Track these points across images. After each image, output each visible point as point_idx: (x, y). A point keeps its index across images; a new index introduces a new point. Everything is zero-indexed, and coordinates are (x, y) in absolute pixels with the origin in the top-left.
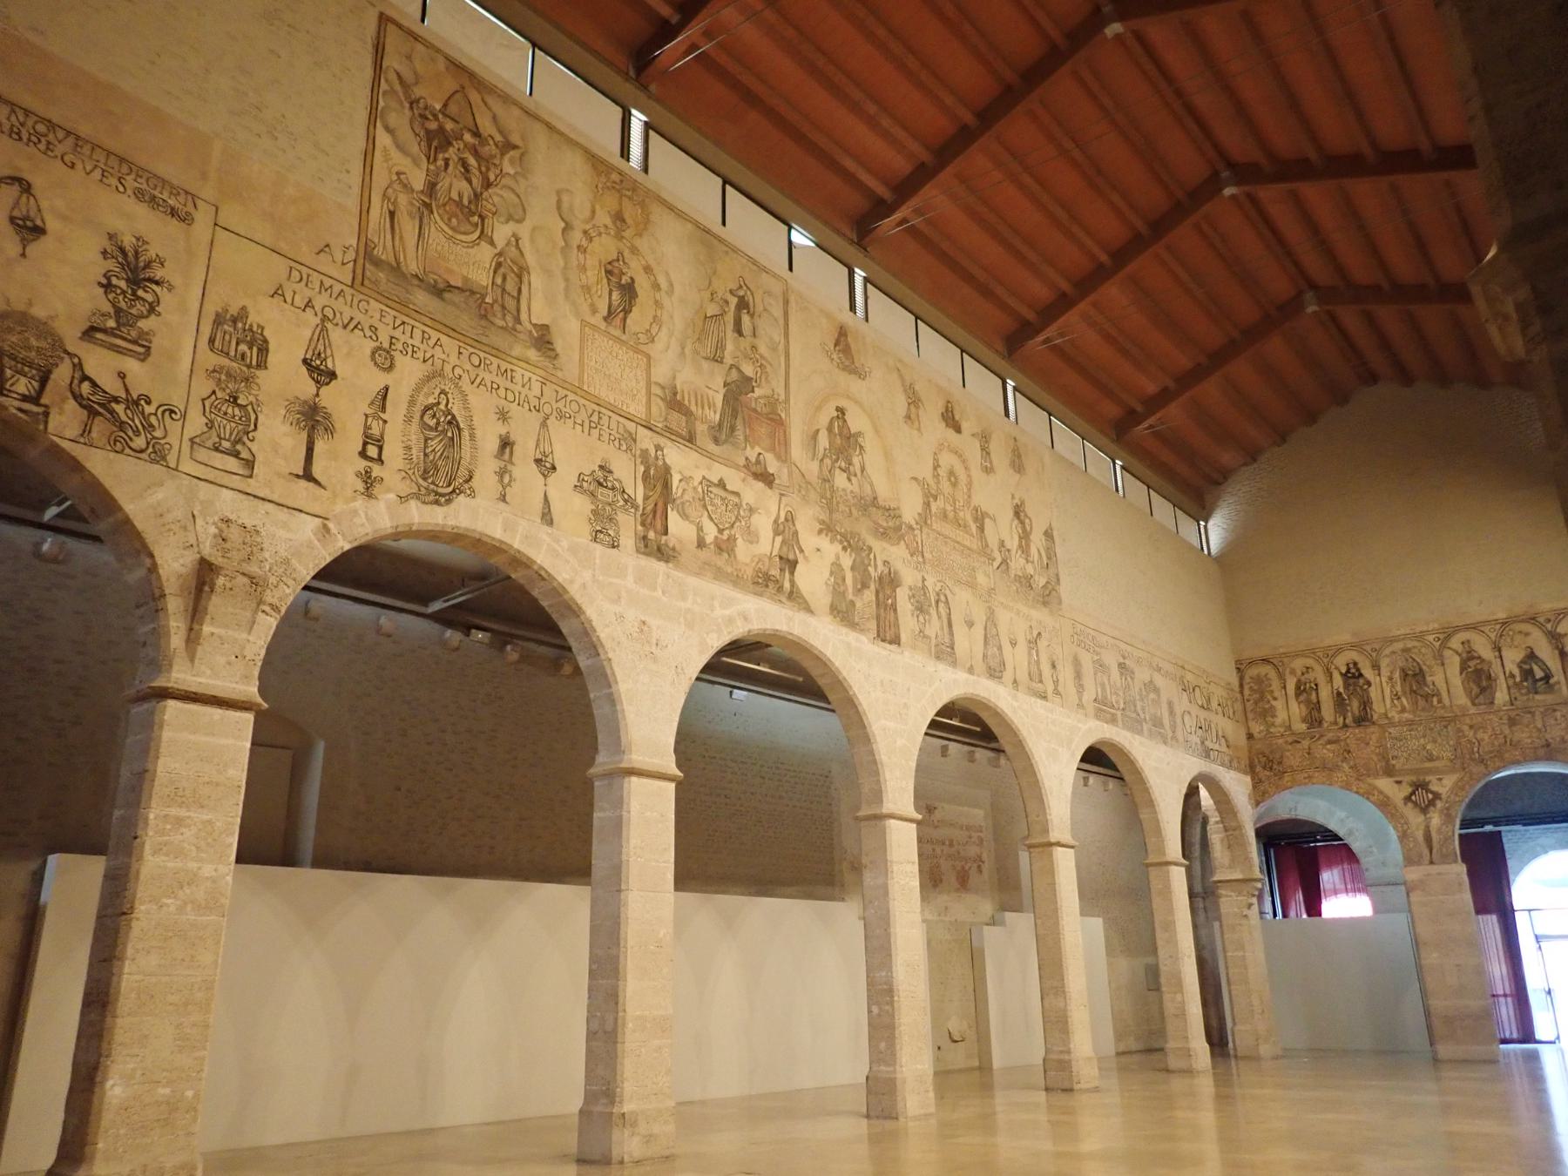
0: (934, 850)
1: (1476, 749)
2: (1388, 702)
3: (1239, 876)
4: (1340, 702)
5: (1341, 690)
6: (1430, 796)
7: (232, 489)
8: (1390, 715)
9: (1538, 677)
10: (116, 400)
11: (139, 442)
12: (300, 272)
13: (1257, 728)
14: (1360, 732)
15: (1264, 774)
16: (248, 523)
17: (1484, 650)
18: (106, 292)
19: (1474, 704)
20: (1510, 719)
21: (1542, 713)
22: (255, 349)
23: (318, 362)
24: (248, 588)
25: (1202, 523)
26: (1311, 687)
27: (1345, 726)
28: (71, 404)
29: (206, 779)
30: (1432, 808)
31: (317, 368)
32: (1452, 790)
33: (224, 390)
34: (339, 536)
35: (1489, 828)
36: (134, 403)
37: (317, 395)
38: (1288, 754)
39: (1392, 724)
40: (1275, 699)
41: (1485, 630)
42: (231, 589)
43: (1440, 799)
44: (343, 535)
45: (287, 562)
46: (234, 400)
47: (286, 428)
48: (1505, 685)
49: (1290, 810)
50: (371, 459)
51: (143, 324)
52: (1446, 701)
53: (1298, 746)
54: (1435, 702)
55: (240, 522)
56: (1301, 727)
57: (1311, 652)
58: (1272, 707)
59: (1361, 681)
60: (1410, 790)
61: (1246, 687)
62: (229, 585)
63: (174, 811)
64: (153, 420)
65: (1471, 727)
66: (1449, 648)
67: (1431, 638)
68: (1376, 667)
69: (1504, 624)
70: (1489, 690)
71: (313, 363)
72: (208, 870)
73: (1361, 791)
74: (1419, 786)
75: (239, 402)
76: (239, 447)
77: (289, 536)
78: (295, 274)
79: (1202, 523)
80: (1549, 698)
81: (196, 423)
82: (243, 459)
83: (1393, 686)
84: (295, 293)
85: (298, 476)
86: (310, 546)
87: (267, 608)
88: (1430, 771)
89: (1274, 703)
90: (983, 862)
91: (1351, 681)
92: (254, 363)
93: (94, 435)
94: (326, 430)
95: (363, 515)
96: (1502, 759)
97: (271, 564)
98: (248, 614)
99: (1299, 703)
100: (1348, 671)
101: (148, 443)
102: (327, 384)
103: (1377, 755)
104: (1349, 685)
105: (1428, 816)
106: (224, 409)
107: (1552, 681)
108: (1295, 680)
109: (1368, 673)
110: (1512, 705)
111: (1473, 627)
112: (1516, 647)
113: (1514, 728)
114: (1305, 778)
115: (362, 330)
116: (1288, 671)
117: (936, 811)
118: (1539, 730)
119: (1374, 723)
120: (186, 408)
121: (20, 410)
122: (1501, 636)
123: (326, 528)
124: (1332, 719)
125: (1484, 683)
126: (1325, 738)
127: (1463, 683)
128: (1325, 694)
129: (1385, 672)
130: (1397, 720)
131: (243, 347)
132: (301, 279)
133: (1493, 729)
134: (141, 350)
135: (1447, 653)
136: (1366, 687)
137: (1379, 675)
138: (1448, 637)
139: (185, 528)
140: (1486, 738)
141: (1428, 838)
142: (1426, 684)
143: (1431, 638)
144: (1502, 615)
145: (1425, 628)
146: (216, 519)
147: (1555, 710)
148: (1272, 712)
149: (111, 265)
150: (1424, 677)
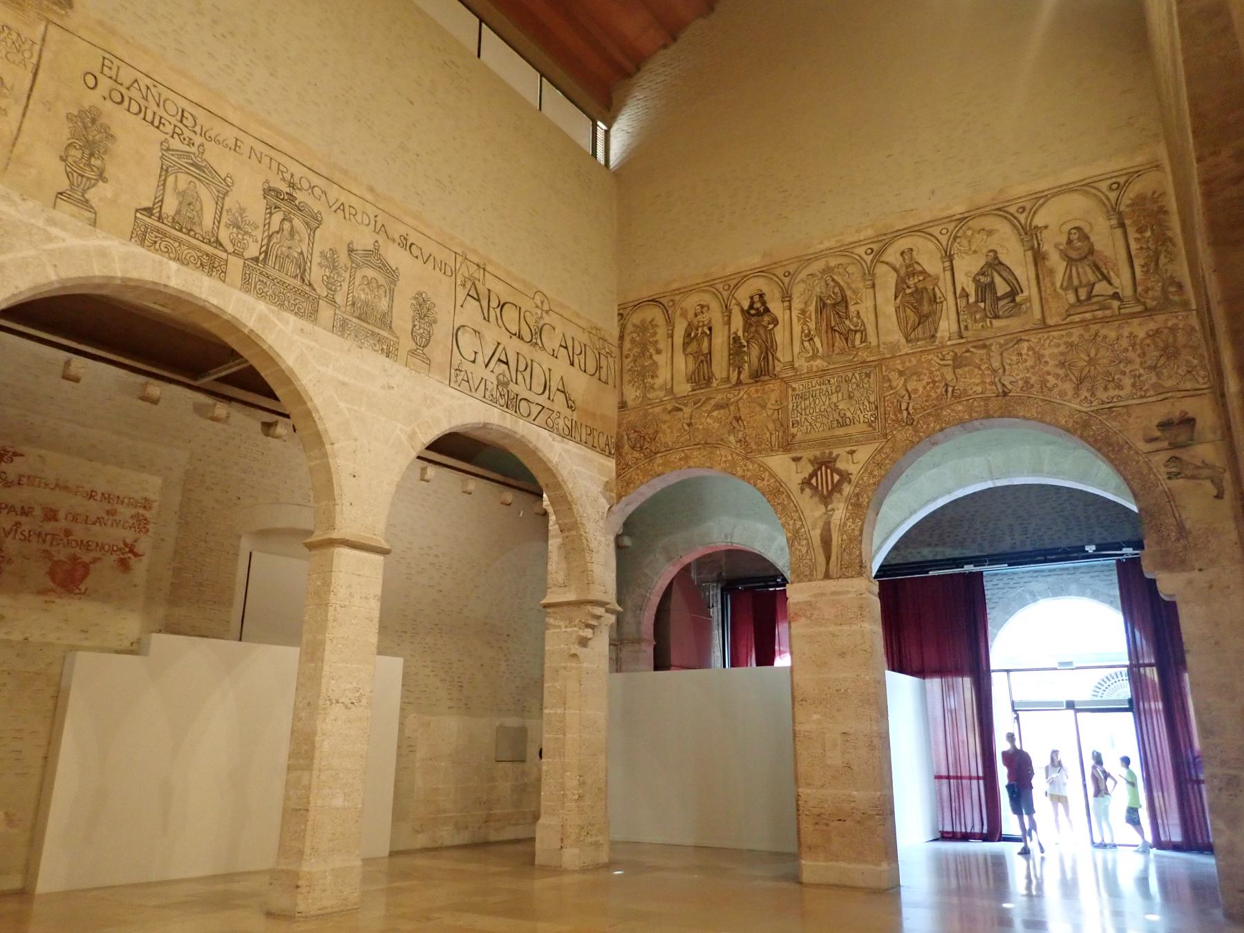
1: (904, 406)
2: (797, 349)
3: (571, 597)
4: (736, 349)
5: (740, 333)
6: (836, 477)
8: (796, 365)
9: (999, 294)
13: (632, 394)
14: (757, 391)
15: (631, 456)
17: (931, 262)
19: (908, 341)
20: (955, 358)
21: (1001, 346)
25: (601, 126)
26: (703, 332)
27: (739, 382)
30: (836, 495)
32: (865, 467)
35: (969, 568)
38: (664, 427)
39: (798, 376)
40: (659, 352)
41: (935, 231)
43: (850, 482)
48: (953, 309)
49: (726, 537)
52: (872, 339)
53: (680, 414)
54: (857, 342)
56: (684, 388)
57: (709, 285)
58: (655, 363)
59: (766, 318)
60: (810, 469)
61: (627, 339)
65: (901, 373)
66: (883, 262)
67: (861, 251)
68: (787, 297)
69: (960, 220)
70: (930, 319)
73: (749, 474)
74: (822, 464)
79: (601, 126)
80: (1014, 324)
83: (805, 323)
88: (840, 441)
89: (655, 357)
90: (136, 555)
91: (754, 319)
96: (938, 417)
99: (686, 355)
100: (751, 307)
103: (774, 421)
104: (751, 325)
105: (830, 507)
107: (1018, 299)
108: (685, 324)
109: (776, 307)
110: (962, 338)
111: (918, 230)
112: (975, 252)
113: (959, 371)
114: (680, 459)
116: (678, 312)
117: (17, 459)
118: (995, 371)
119: (775, 377)
122: (955, 238)
124: (724, 375)
125: (926, 308)
126: (713, 402)
127: (897, 309)
128: (720, 341)
129: (797, 305)
130: (805, 371)
133: (931, 372)
135: (881, 269)
136: (771, 326)
137: (790, 309)
138: (882, 251)
140: (921, 390)
141: (826, 542)
142: (847, 317)
143: (861, 251)
144: (959, 209)
145: (855, 239)
147: (1020, 340)
148: (653, 370)
150: (847, 307)
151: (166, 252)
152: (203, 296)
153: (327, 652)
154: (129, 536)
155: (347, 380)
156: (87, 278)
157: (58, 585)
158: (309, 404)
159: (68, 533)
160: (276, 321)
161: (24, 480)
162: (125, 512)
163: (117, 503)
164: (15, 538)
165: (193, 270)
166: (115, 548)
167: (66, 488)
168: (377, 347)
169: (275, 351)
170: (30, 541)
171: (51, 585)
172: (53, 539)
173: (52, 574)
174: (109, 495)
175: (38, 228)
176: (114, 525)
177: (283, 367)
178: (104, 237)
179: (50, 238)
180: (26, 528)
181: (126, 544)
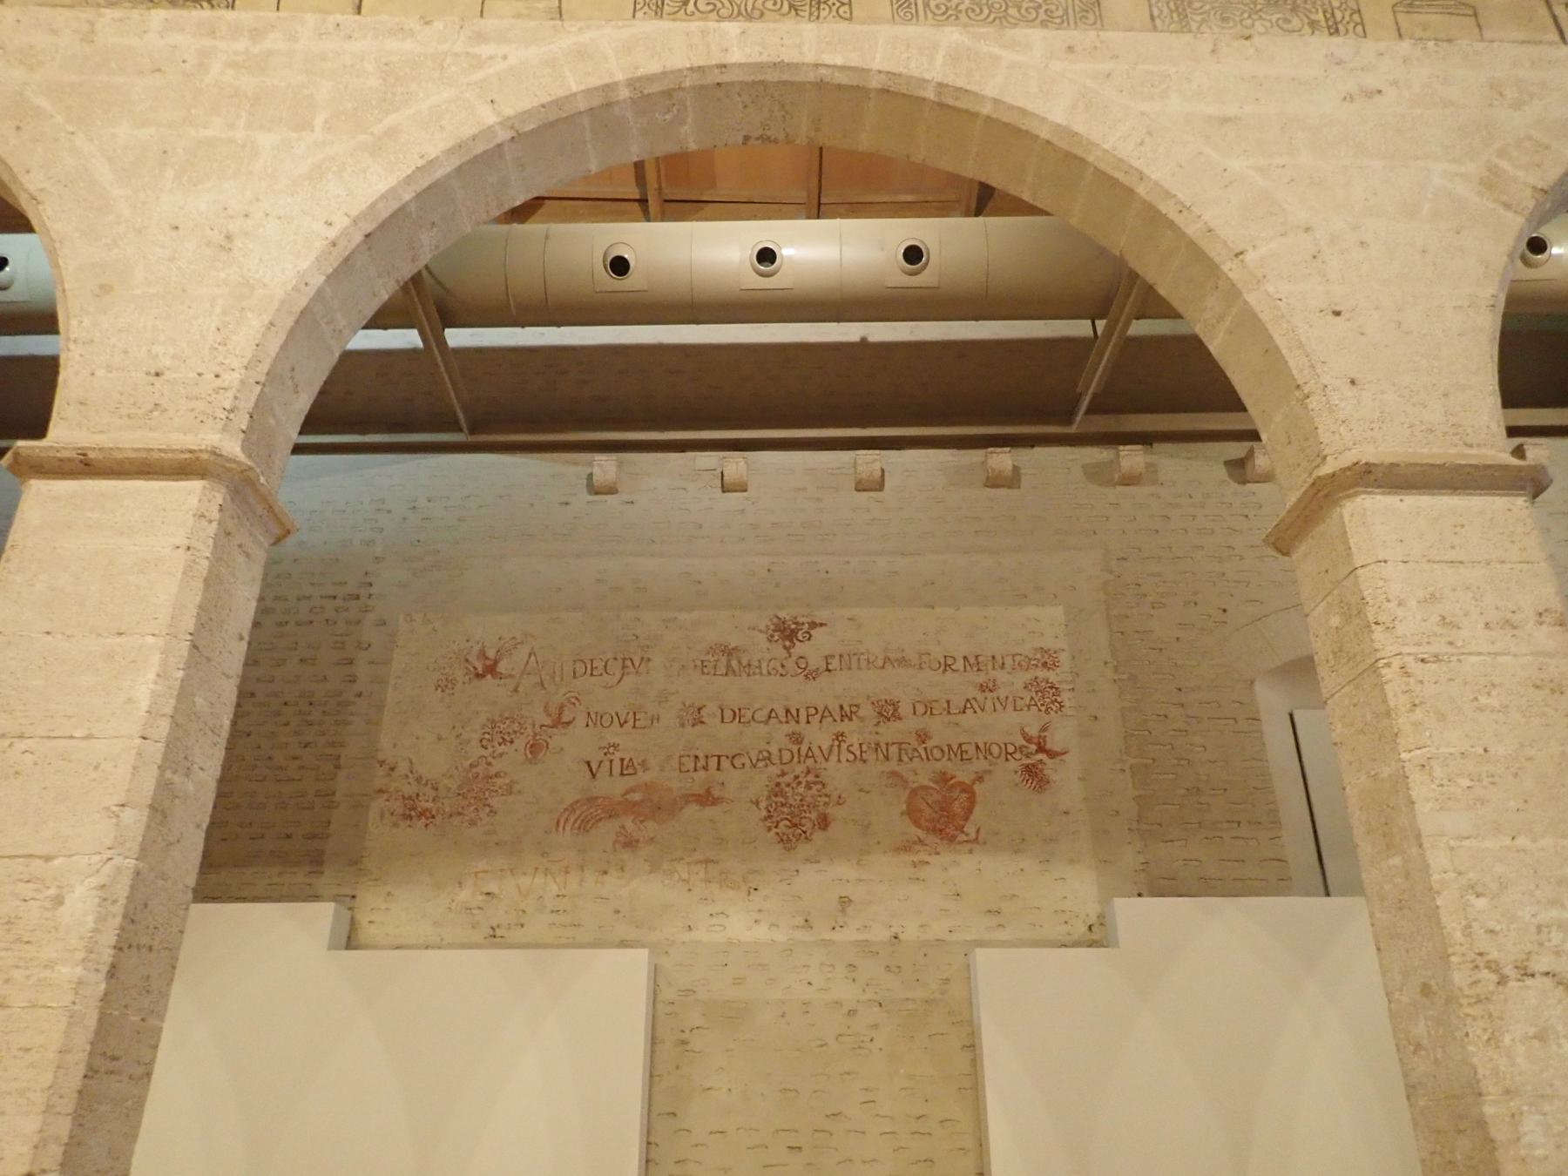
0: (797, 738)
90: (1052, 755)
151: (712, 11)
152: (810, 58)
153: (1423, 809)
154: (1032, 722)
155: (1232, 110)
156: (557, 103)
157: (928, 830)
158: (1141, 190)
159: (923, 737)
160: (996, 50)
161: (835, 664)
162: (1013, 682)
163: (994, 668)
164: (839, 761)
165: (775, 21)
166: (1011, 749)
167: (903, 662)
168: (1296, 23)
169: (1011, 107)
170: (865, 761)
171: (914, 832)
172: (900, 750)
173: (912, 813)
174: (977, 657)
175: (456, 55)
176: (998, 706)
177: (1044, 134)
178: (580, 29)
179: (477, 63)
180: (854, 739)
181: (1029, 740)
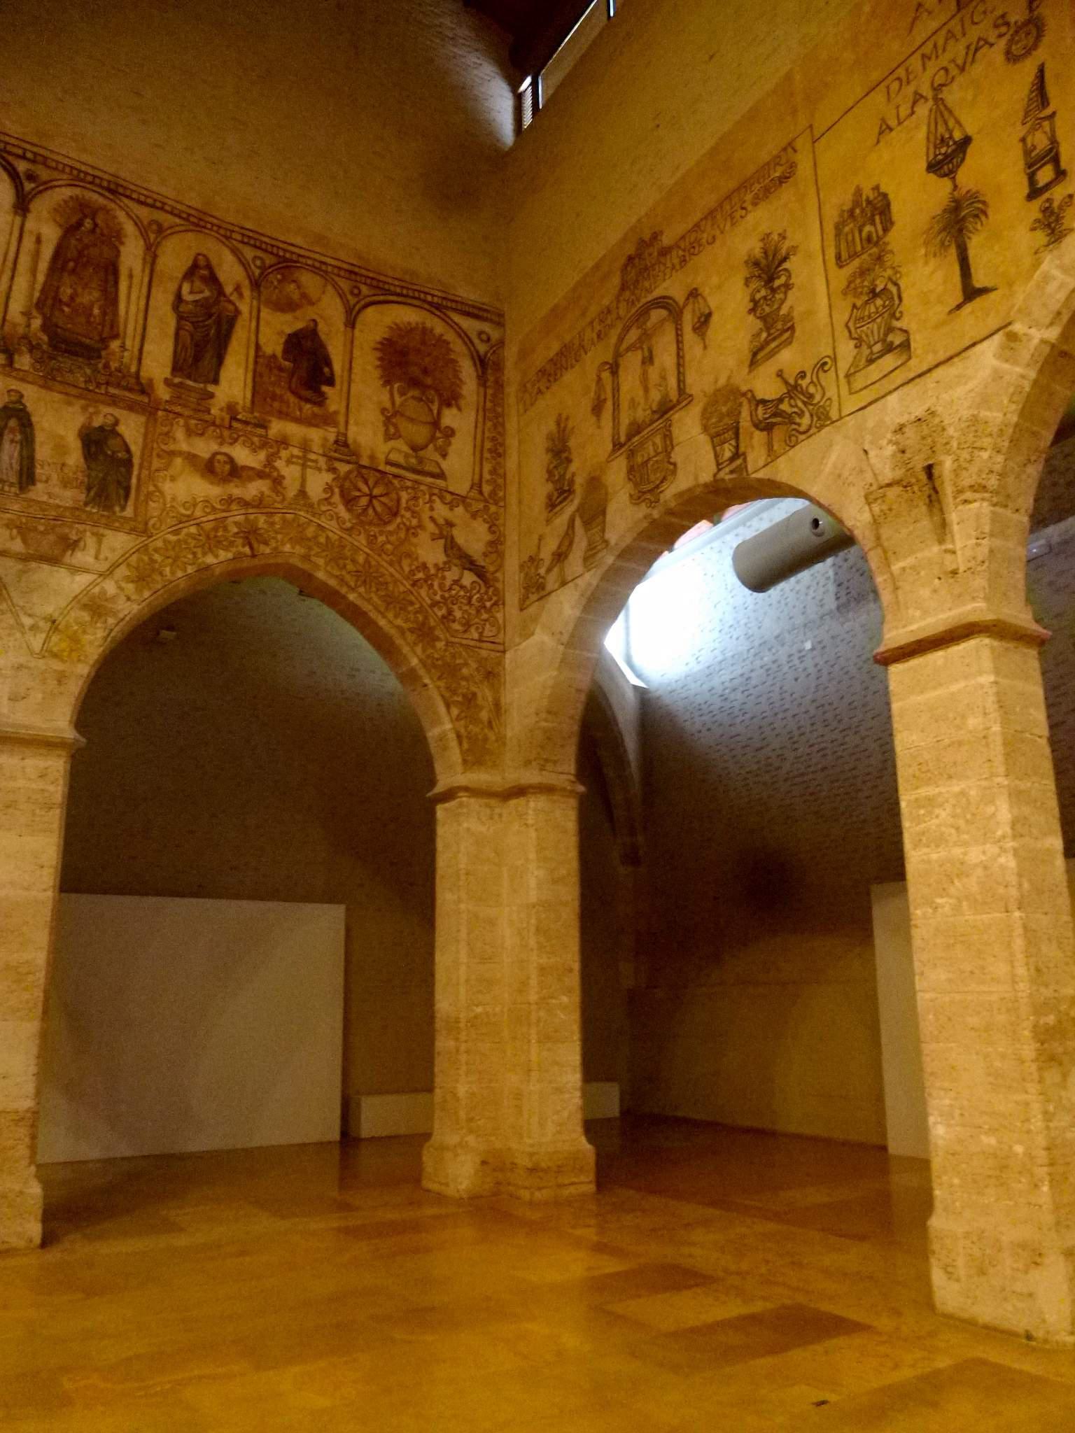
7: (896, 389)
10: (781, 400)
11: (805, 421)
12: (899, 79)
16: (919, 411)
18: (755, 315)
22: (877, 218)
23: (943, 150)
24: (906, 496)
28: (757, 433)
29: (947, 741)
31: (946, 156)
33: (861, 293)
34: (1033, 331)
36: (793, 390)
37: (955, 187)
42: (890, 510)
44: (1034, 324)
45: (974, 420)
46: (874, 294)
47: (933, 263)
50: (1048, 186)
51: (783, 311)
55: (913, 418)
62: (885, 507)
63: (924, 791)
64: (812, 390)
71: (940, 157)
72: (975, 855)
75: (878, 290)
76: (890, 338)
77: (970, 385)
78: (895, 85)
81: (846, 350)
82: (899, 346)
84: (898, 107)
85: (959, 307)
86: (997, 376)
87: (968, 495)
92: (881, 232)
93: (775, 448)
94: (977, 216)
95: (1056, 273)
97: (958, 439)
98: (926, 523)
101: (812, 416)
102: (963, 160)
106: (867, 313)
115: (986, 42)
120: (834, 349)
121: (732, 472)
123: (1013, 337)
131: (868, 228)
132: (901, 85)
134: (787, 335)
139: (861, 471)
146: (889, 436)
149: (755, 284)
